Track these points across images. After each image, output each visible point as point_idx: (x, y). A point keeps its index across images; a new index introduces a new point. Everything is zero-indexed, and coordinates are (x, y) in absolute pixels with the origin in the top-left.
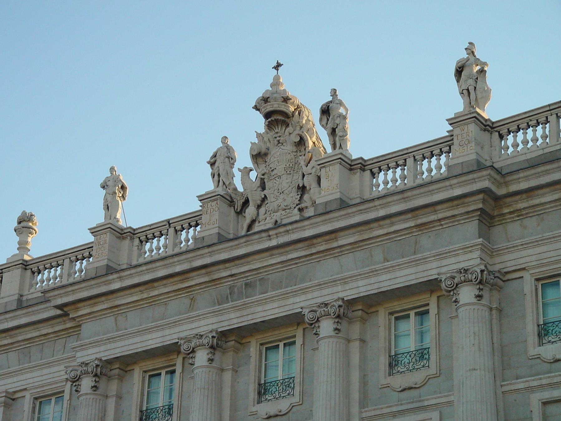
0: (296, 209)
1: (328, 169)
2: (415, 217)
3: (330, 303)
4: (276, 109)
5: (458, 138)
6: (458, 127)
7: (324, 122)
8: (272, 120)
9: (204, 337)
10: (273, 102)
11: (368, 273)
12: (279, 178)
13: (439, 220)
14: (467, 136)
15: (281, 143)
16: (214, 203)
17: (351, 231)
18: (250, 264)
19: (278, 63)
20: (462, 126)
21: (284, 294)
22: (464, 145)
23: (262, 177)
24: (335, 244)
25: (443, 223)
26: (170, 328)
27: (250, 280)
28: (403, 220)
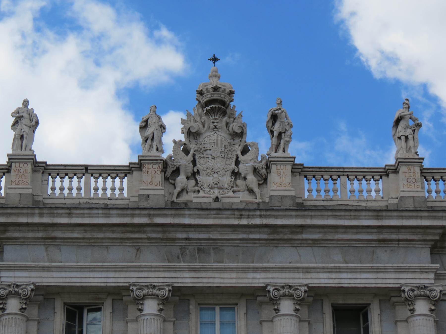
0: (231, 191)
1: (279, 167)
2: (380, 233)
3: (295, 286)
4: (222, 99)
6: (405, 166)
7: (270, 124)
8: (216, 107)
9: (157, 288)
10: (221, 92)
11: (331, 268)
12: (213, 159)
13: (399, 240)
15: (217, 128)
16: (156, 166)
17: (318, 230)
18: (209, 233)
19: (214, 56)
20: (409, 167)
21: (245, 268)
22: (412, 183)
23: (195, 153)
24: (299, 237)
25: (400, 243)
26: (115, 271)
28: (367, 233)
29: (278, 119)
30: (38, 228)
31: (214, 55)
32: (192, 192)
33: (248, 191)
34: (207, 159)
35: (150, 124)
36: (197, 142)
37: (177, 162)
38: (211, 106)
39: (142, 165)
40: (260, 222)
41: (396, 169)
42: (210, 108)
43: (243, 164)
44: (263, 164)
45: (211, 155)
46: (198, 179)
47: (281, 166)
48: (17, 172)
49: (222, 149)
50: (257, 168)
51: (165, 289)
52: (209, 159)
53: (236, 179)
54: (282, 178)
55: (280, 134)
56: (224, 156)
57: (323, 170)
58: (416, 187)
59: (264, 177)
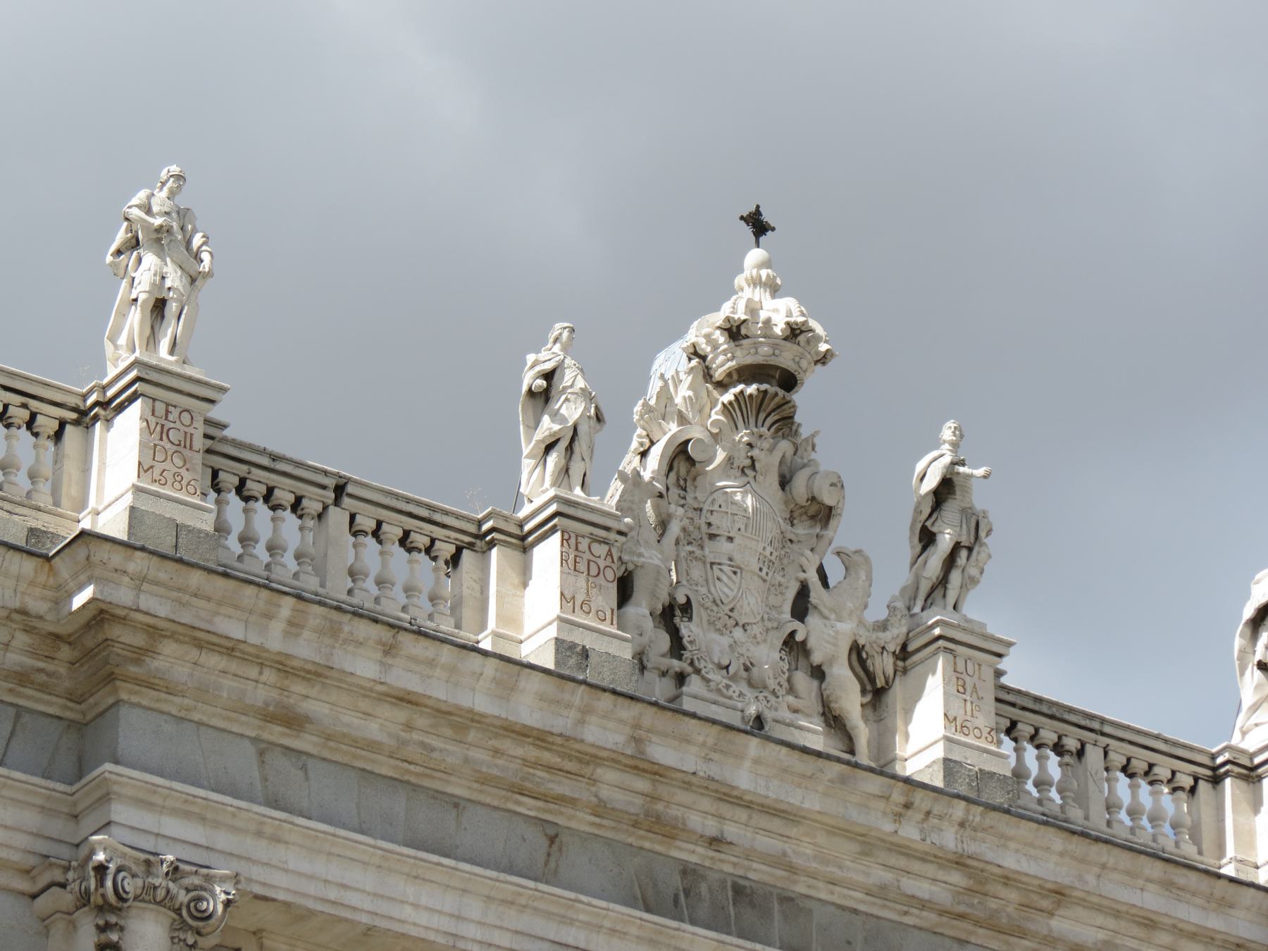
12: (735, 573)
27: (753, 884)
30: (261, 673)
31: (758, 207)
32: (656, 671)
33: (823, 718)
34: (715, 567)
35: (565, 388)
36: (684, 498)
37: (632, 553)
40: (957, 846)
42: (755, 393)
43: (826, 618)
44: (893, 638)
45: (730, 559)
46: (684, 631)
47: (966, 661)
48: (156, 435)
50: (863, 646)
52: (721, 570)
54: (969, 704)
56: (767, 574)
57: (1045, 709)
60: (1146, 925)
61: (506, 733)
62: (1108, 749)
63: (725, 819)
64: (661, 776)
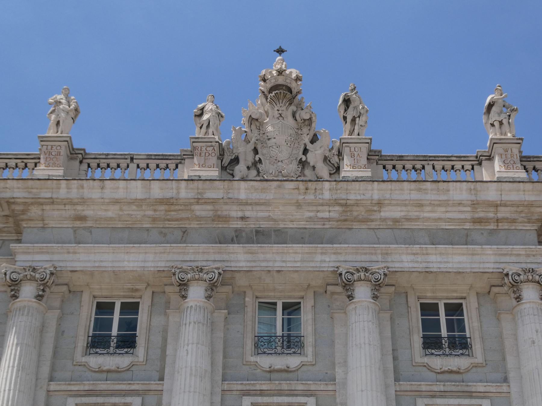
5: (503, 157)
12: (277, 147)
14: (511, 157)
15: (282, 117)
27: (263, 229)
29: (351, 103)
30: (65, 207)
35: (205, 111)
36: (260, 132)
38: (276, 92)
39: (194, 147)
41: (490, 156)
44: (335, 151)
46: (260, 169)
48: (48, 154)
49: (287, 138)
51: (214, 272)
52: (273, 148)
53: (303, 168)
54: (356, 160)
55: (354, 120)
56: (290, 145)
58: (515, 168)
59: (336, 165)
60: (419, 206)
61: (156, 203)
62: (434, 165)
63: (244, 211)
64: (215, 203)
